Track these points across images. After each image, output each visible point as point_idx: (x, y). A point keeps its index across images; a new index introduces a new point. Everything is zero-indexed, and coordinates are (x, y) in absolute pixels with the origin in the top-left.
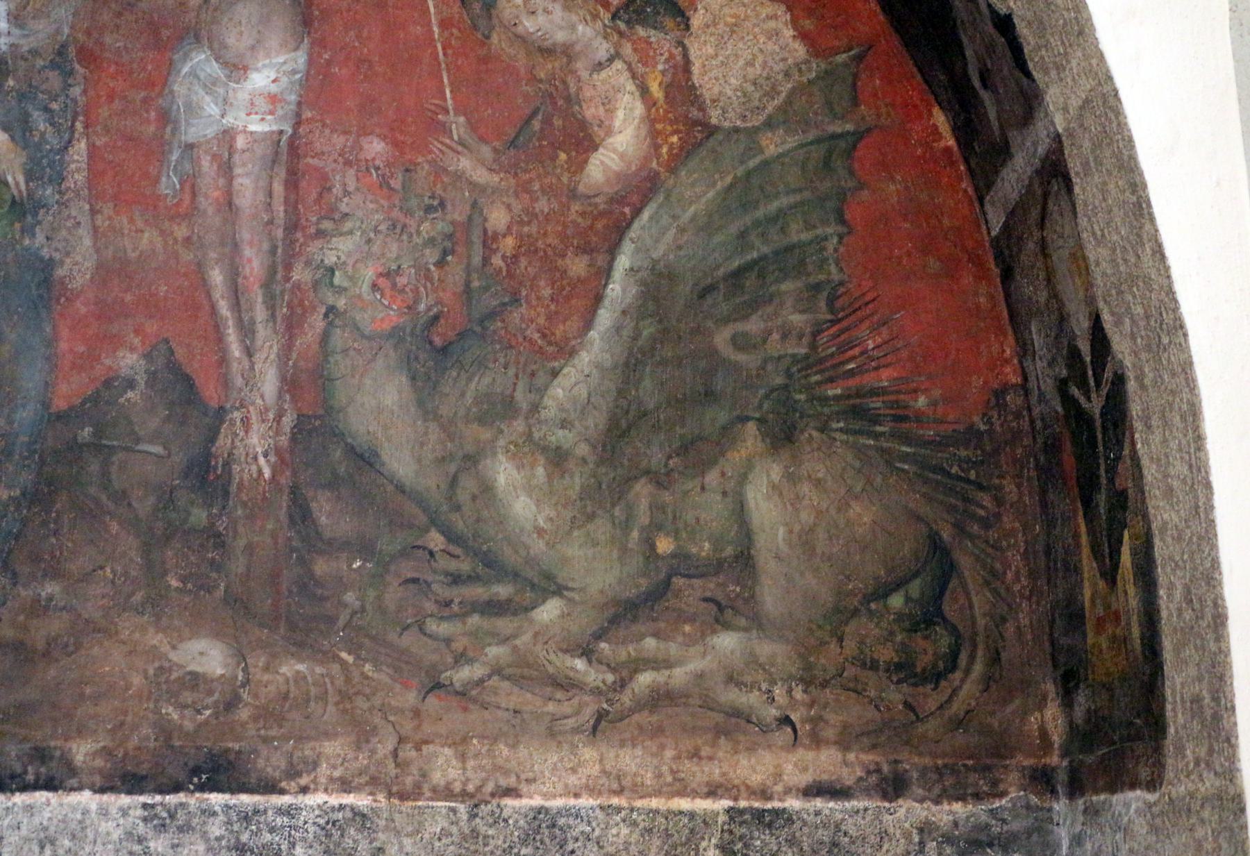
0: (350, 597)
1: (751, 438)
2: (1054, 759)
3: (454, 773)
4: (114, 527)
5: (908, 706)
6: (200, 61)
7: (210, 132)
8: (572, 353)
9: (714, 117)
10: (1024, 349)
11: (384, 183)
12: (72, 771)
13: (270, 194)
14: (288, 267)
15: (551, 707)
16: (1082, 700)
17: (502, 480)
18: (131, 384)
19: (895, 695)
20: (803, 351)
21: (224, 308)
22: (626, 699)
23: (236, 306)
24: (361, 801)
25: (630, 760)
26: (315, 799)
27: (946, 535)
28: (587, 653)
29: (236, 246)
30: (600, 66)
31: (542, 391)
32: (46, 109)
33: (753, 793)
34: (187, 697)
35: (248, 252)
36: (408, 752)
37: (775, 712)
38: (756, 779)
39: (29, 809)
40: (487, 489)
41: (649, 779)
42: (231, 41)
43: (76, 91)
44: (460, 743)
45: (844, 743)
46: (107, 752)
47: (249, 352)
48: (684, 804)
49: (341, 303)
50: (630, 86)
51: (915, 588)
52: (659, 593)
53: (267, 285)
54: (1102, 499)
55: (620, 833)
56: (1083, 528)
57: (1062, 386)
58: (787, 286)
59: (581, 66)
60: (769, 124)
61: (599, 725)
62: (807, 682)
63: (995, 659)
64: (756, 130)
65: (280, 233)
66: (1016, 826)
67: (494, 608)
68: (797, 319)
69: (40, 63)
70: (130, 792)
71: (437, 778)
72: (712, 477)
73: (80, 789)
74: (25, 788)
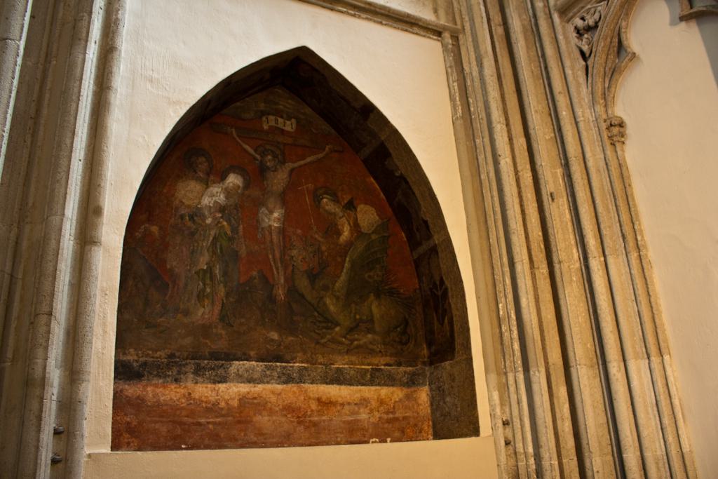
0: (301, 325)
1: (372, 297)
2: (426, 360)
3: (322, 360)
4: (254, 308)
5: (402, 350)
6: (263, 210)
7: (267, 225)
8: (339, 277)
9: (362, 230)
10: (420, 281)
11: (301, 239)
12: (251, 357)
13: (279, 240)
14: (284, 256)
15: (339, 348)
16: (433, 348)
17: (328, 302)
18: (255, 278)
19: (399, 347)
20: (381, 279)
21: (272, 263)
22: (352, 347)
23: (275, 263)
24: (306, 365)
25: (353, 358)
26: (297, 364)
27: (407, 317)
28: (345, 337)
29: (274, 251)
30: (340, 218)
31: (334, 285)
32: (234, 218)
33: (375, 365)
34: (272, 343)
35: (276, 252)
36: (313, 356)
37: (378, 350)
38: (376, 362)
39: (243, 364)
40: (325, 304)
41: (357, 362)
42: (269, 205)
43: (240, 214)
44: (323, 355)
45: (391, 356)
46: (257, 354)
47: (278, 273)
48: (363, 367)
49: (295, 264)
50: (347, 223)
51: (402, 327)
52: (357, 326)
53: (280, 259)
54: (440, 311)
55: (352, 372)
56: (435, 315)
57: (431, 289)
58: (378, 266)
59: (337, 218)
60: (373, 233)
61: (348, 352)
62: (384, 344)
63: (416, 341)
64: (370, 234)
65: (282, 248)
66: (420, 371)
67: (327, 328)
68: (380, 273)
69: (232, 207)
70: (262, 362)
71: (319, 361)
72: (366, 304)
73: (252, 361)
74: (242, 360)
